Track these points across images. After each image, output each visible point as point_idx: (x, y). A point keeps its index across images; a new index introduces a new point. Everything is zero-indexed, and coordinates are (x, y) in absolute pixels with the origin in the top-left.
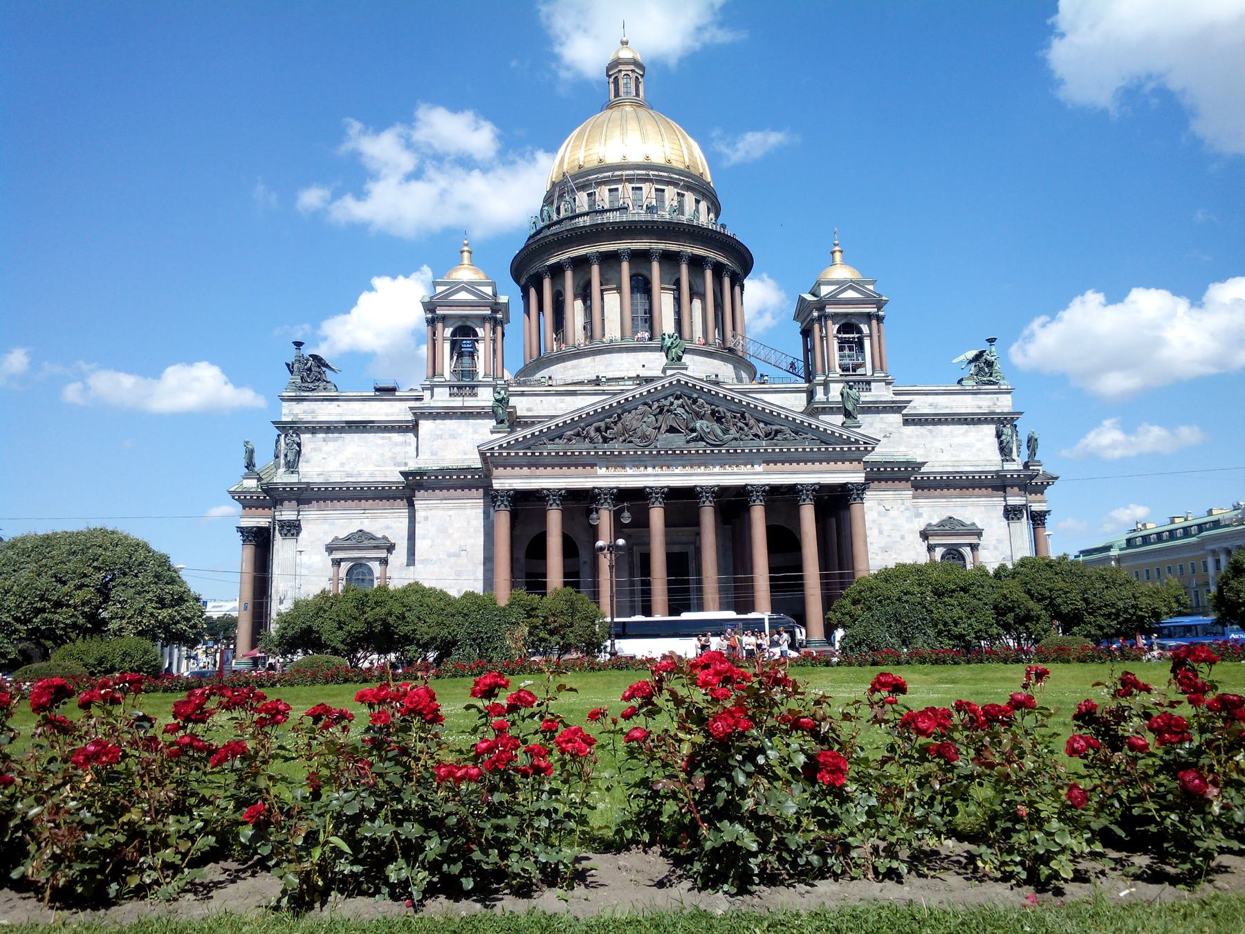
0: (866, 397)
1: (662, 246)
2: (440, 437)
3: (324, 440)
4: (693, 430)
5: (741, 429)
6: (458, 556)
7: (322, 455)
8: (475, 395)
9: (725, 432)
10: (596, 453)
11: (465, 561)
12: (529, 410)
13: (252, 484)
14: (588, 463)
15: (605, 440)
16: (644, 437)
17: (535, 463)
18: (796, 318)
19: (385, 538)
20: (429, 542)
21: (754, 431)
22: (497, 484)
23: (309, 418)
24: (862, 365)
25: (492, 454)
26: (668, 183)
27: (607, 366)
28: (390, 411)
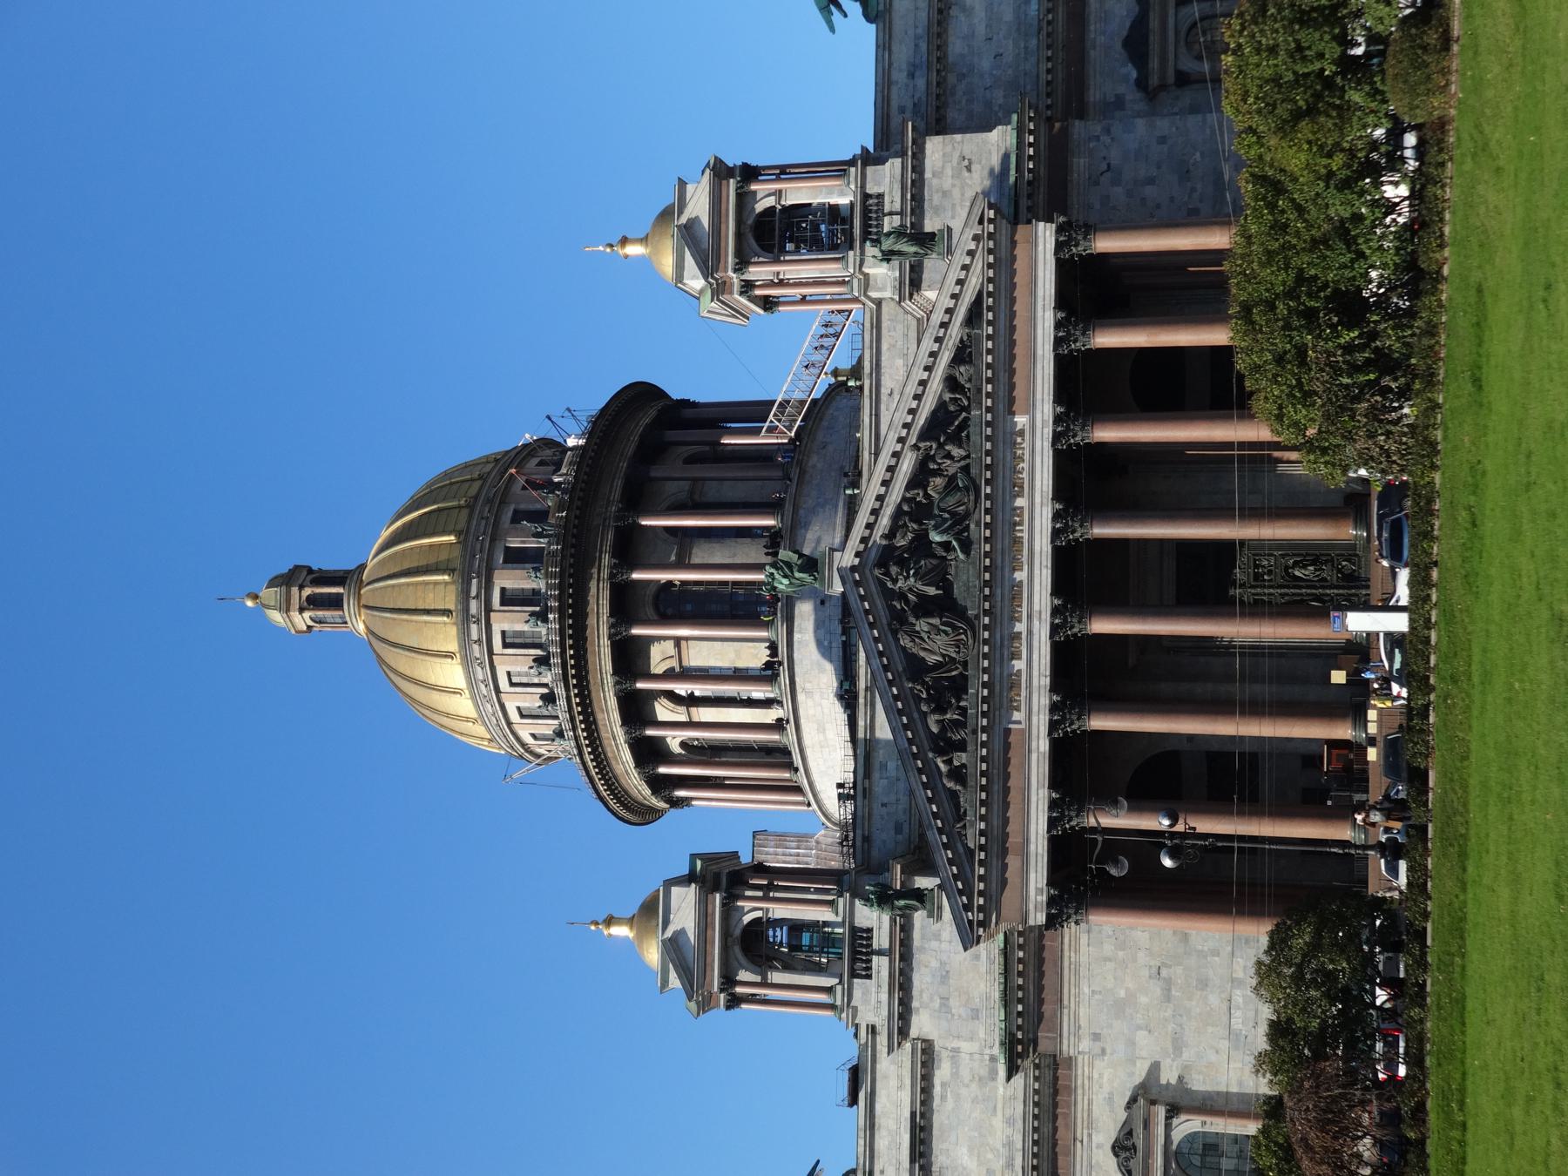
0: (893, 201)
1: (606, 559)
2: (945, 1000)
6: (1168, 985)
8: (870, 930)
10: (984, 730)
11: (1179, 970)
12: (898, 829)
14: (1004, 748)
15: (963, 711)
17: (999, 844)
20: (1142, 1034)
22: (1038, 918)
24: (834, 210)
25: (982, 924)
26: (493, 540)
28: (894, 1083)
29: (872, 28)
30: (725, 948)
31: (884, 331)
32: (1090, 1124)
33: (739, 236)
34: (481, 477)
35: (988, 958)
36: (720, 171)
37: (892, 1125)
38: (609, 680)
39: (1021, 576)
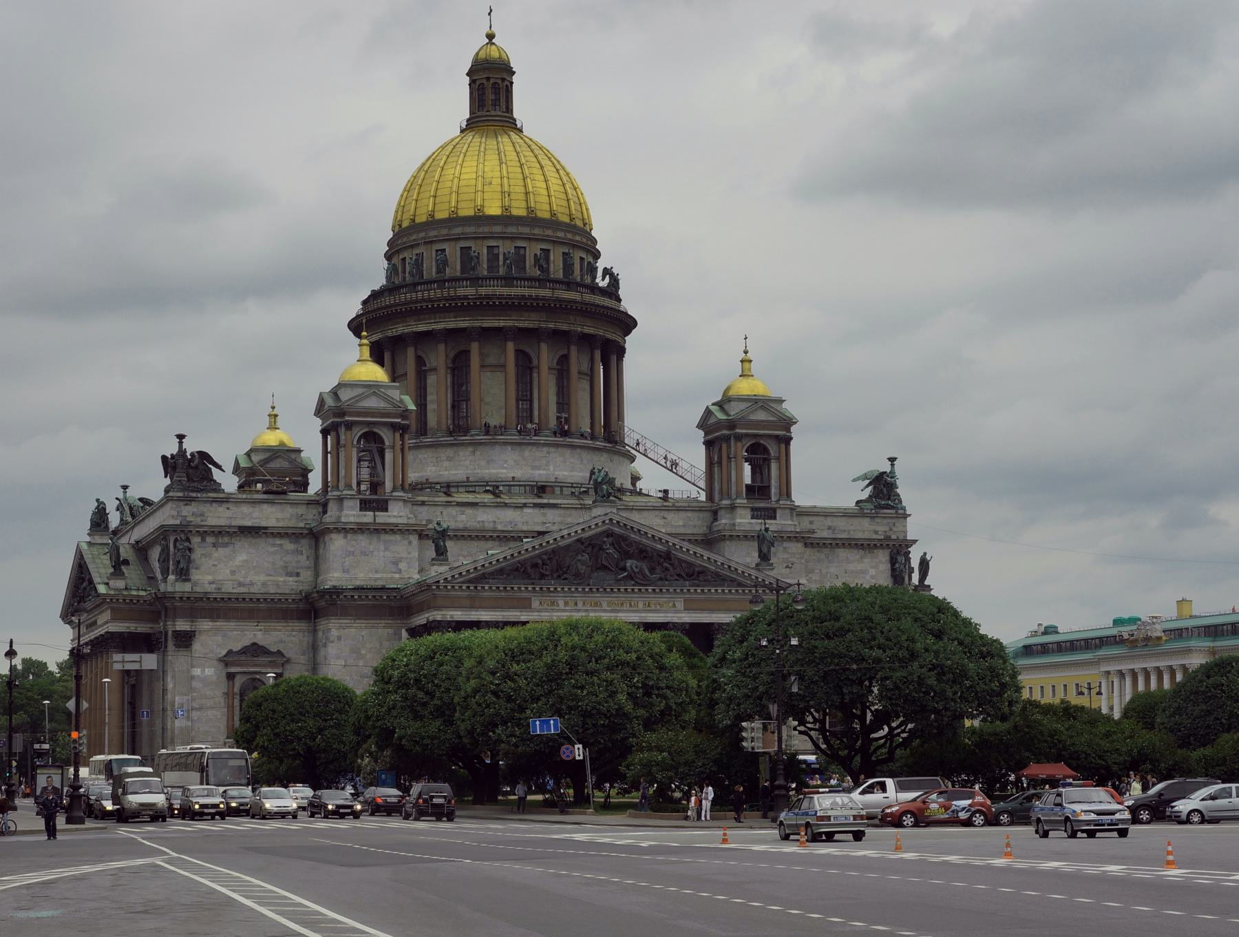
1: (551, 326)
2: (353, 553)
3: (214, 545)
4: (624, 569)
5: (667, 569)
7: (211, 562)
8: (386, 510)
9: (652, 570)
13: (120, 584)
15: (542, 576)
16: (578, 575)
18: (701, 426)
19: (279, 653)
21: (678, 570)
23: (198, 521)
25: (438, 587)
27: (488, 462)
28: (280, 515)
29: (852, 504)
30: (369, 423)
31: (697, 514)
32: (266, 631)
33: (755, 436)
34: (585, 224)
35: (376, 580)
36: (787, 423)
37: (256, 514)
38: (477, 324)
39: (605, 606)
